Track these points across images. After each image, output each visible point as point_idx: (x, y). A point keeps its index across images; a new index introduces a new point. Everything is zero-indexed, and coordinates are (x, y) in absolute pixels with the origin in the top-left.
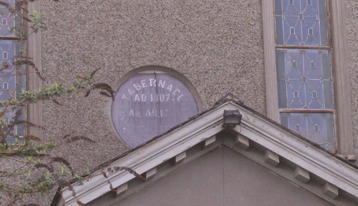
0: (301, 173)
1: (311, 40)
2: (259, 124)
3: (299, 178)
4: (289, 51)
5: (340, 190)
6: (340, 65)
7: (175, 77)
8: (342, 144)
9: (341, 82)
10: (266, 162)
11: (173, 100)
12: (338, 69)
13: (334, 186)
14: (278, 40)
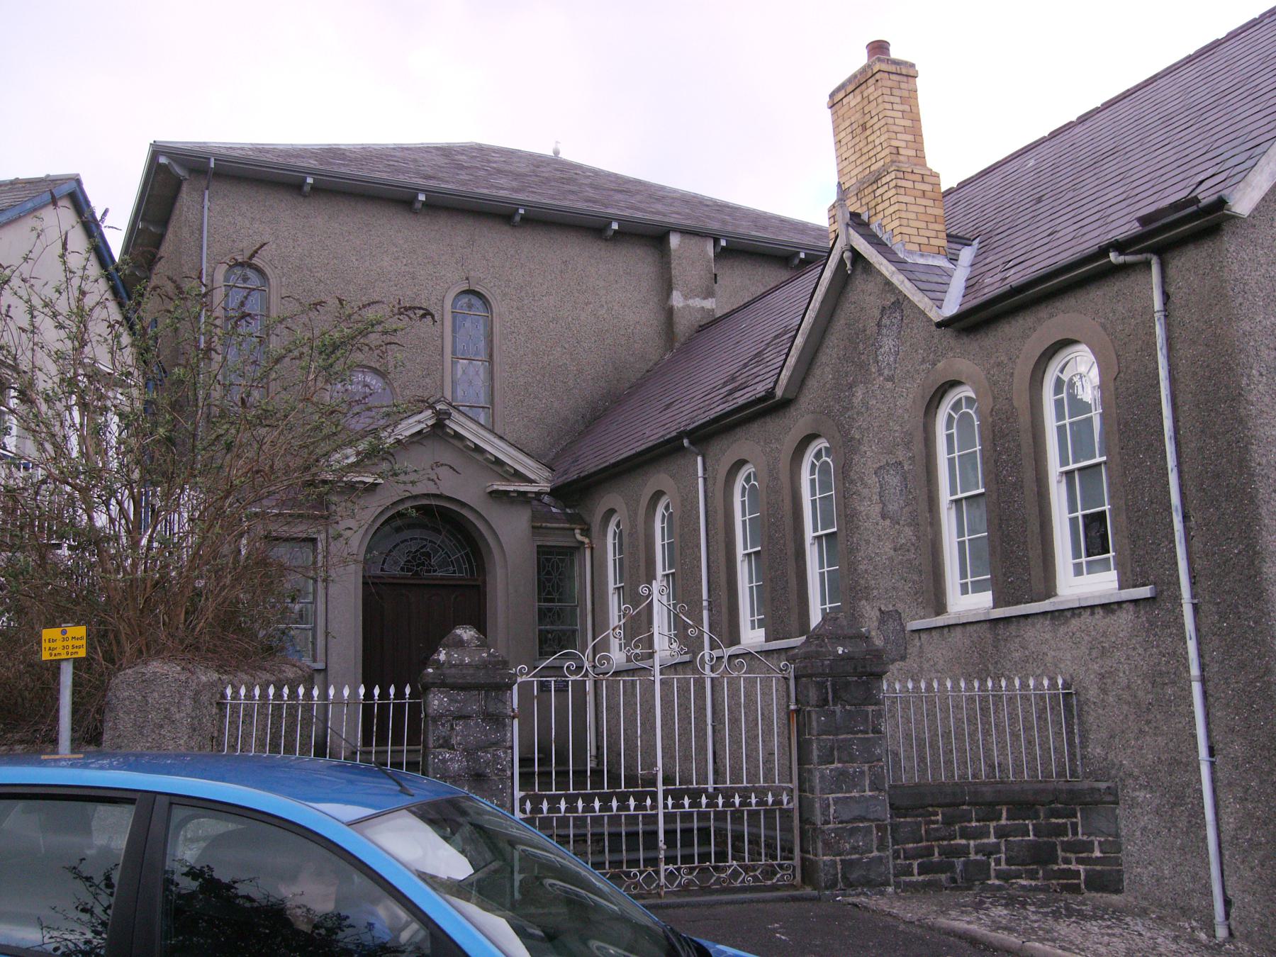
0: (489, 456)
1: (475, 355)
2: (462, 419)
3: (487, 459)
4: (461, 361)
5: (515, 470)
6: (497, 375)
7: (379, 375)
8: (496, 426)
9: (497, 386)
10: (484, 459)
11: (840, 652)
12: (495, 378)
13: (512, 467)
14: (454, 353)
